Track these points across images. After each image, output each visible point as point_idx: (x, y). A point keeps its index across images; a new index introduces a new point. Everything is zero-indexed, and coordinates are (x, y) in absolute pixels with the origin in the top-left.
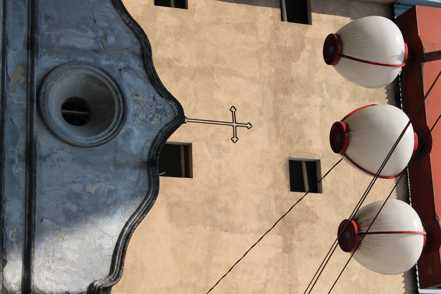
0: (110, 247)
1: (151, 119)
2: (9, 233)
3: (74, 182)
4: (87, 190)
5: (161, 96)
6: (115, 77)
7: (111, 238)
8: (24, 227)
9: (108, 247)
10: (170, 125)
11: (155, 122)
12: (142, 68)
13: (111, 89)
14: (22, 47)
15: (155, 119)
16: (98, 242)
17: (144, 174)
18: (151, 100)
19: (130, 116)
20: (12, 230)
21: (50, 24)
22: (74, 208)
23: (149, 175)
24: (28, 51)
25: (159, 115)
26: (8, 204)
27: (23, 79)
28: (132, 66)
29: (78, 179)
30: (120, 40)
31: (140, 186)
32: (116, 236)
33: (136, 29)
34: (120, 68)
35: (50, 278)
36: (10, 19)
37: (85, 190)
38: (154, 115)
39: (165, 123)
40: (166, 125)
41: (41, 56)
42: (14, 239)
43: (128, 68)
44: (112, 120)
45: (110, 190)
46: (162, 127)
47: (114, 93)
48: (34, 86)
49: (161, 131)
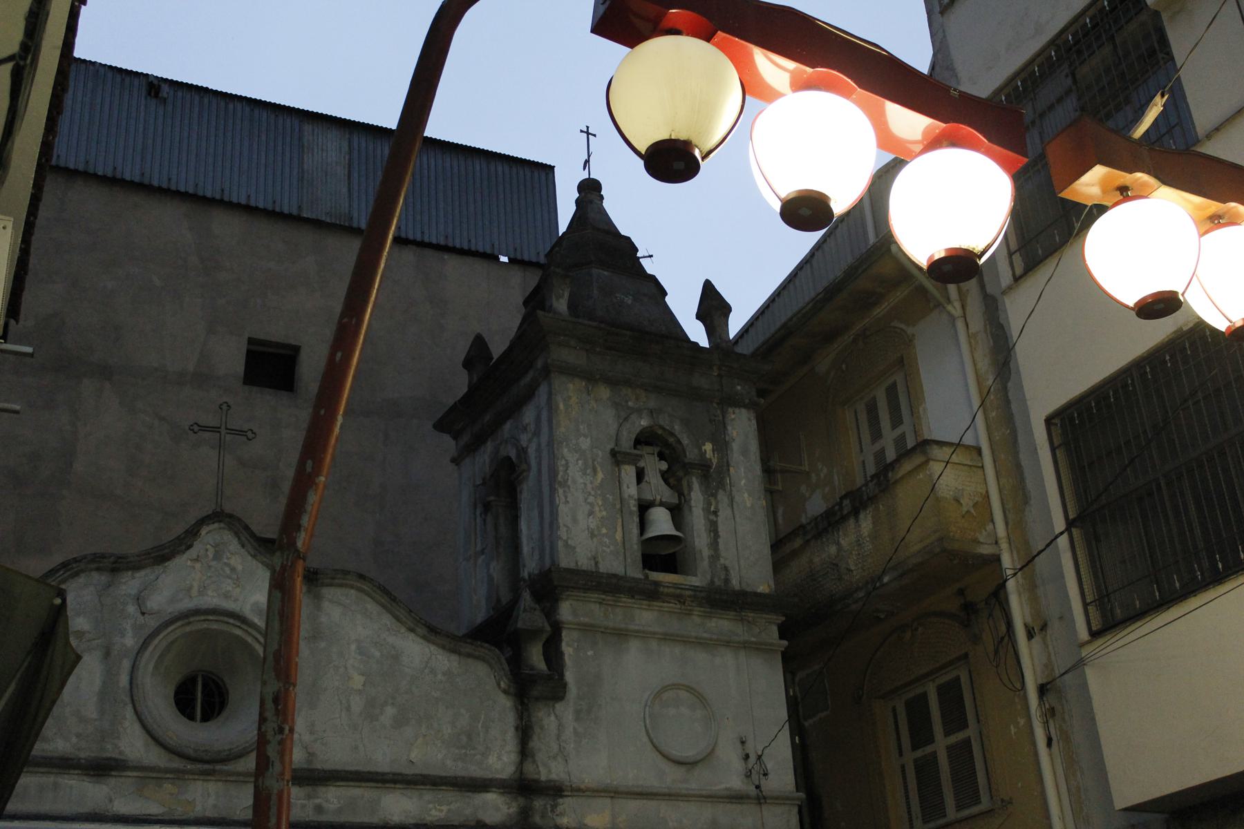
0: (446, 659)
1: (233, 569)
2: (436, 816)
3: (348, 709)
4: (361, 688)
5: (189, 547)
6: (158, 624)
7: (433, 656)
8: (425, 792)
9: (446, 662)
10: (243, 539)
11: (236, 561)
12: (137, 575)
13: (179, 633)
14: (104, 787)
15: (232, 562)
16: (440, 677)
17: (328, 592)
18: (198, 565)
19: (229, 605)
20: (430, 810)
21: (55, 734)
22: (390, 711)
23: (331, 585)
24: (112, 776)
25: (225, 556)
26: (390, 817)
27: (168, 786)
28: (134, 592)
29: (343, 702)
30: (83, 606)
31: (348, 601)
32: (430, 649)
33: (61, 575)
34: (139, 615)
35: (498, 754)
36: (46, 808)
37: (360, 692)
38: (225, 563)
39: (239, 547)
40: (243, 546)
41: (121, 753)
42: (443, 808)
43: (139, 600)
44: (237, 637)
45: (358, 651)
46: (246, 553)
47: (188, 629)
48: (185, 768)
49: (254, 556)
